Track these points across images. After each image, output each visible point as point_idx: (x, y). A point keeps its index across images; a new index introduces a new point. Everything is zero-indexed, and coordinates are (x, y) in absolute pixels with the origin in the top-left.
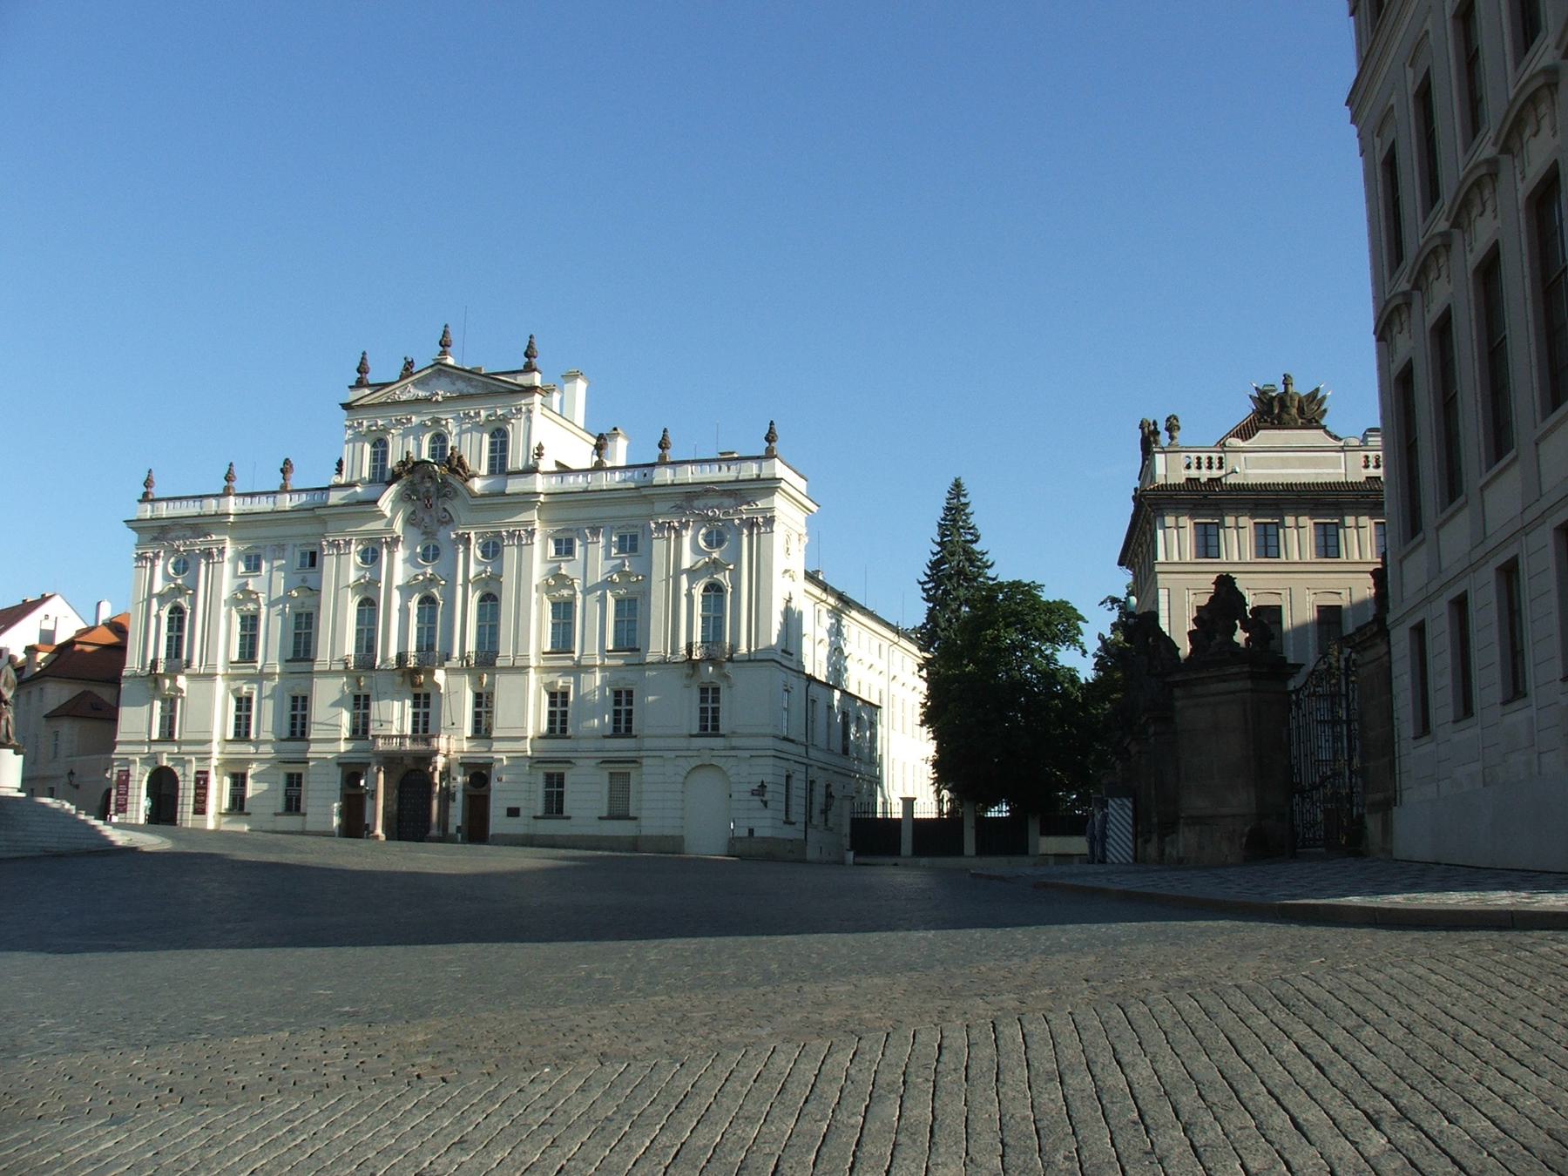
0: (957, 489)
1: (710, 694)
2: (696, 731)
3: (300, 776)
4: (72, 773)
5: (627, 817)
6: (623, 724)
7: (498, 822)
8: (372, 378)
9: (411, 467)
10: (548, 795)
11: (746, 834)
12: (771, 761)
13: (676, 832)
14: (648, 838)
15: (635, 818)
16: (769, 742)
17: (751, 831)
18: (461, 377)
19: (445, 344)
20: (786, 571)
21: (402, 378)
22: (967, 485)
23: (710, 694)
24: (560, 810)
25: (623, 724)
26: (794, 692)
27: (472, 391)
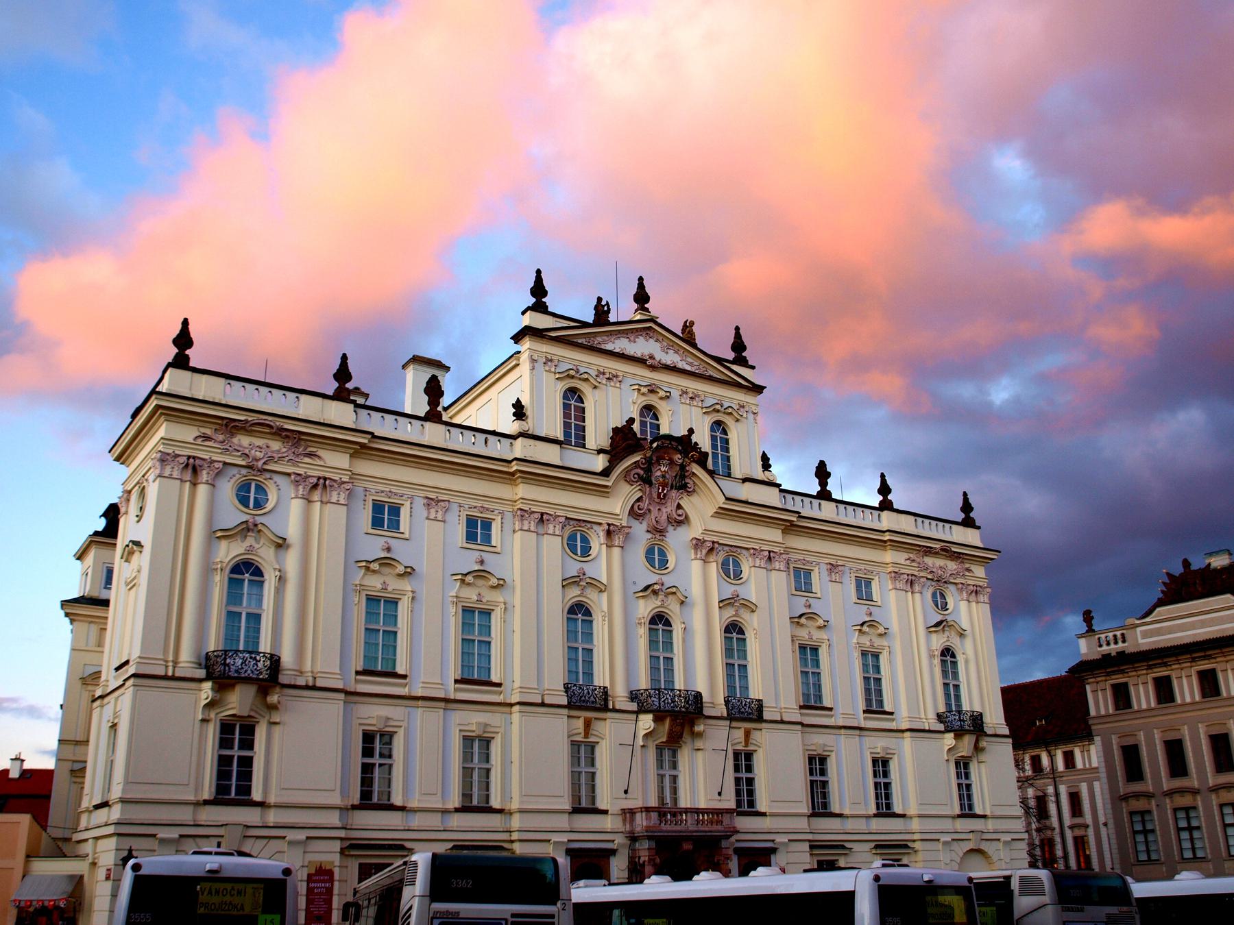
2: (957, 811)
19: (641, 298)
27: (688, 368)
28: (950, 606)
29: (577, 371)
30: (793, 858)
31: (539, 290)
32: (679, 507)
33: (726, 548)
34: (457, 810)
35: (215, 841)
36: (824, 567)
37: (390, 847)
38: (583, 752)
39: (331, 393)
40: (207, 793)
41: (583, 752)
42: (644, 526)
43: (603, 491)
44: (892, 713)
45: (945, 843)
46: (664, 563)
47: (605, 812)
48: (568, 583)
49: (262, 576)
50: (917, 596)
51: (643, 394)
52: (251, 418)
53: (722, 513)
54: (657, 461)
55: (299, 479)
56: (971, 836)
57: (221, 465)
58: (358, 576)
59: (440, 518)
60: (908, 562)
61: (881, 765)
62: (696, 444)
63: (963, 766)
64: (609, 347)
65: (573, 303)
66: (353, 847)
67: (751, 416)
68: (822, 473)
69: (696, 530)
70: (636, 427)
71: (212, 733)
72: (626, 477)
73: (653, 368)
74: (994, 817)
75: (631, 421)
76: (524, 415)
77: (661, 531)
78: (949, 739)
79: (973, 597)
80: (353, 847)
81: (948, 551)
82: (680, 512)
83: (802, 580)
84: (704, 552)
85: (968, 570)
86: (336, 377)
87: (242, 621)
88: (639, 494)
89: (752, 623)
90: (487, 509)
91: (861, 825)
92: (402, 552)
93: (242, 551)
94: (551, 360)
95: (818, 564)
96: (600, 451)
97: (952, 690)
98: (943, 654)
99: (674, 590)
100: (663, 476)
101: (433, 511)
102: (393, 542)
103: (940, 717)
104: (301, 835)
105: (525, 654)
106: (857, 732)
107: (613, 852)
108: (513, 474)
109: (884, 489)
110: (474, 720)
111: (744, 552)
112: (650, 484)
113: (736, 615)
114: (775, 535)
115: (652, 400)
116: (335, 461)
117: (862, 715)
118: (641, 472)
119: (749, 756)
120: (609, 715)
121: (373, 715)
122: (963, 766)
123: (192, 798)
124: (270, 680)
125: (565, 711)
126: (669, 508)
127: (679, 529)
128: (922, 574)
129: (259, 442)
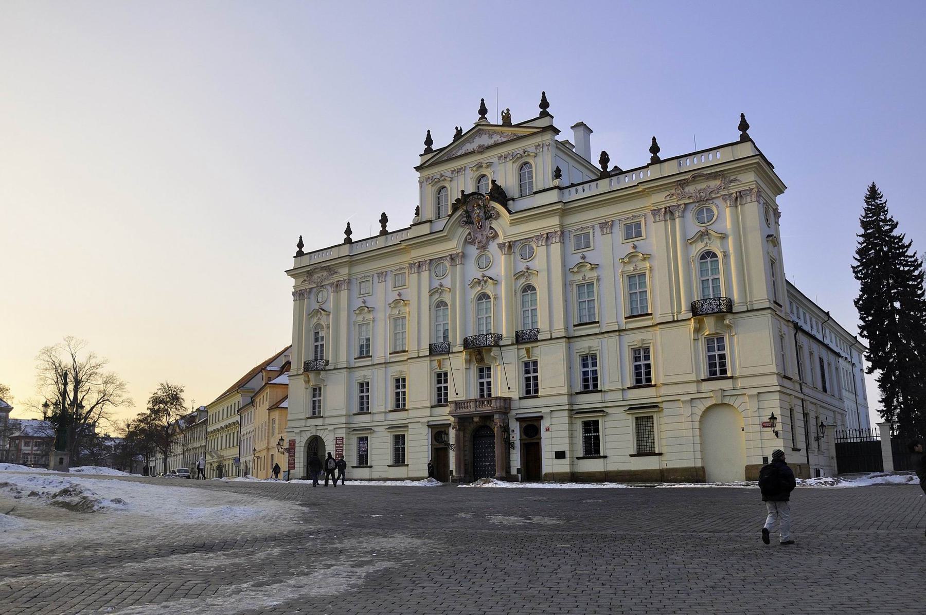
0: (873, 193)
1: (715, 343)
3: (403, 436)
5: (654, 454)
6: (643, 377)
7: (549, 464)
8: (434, 147)
9: (465, 199)
10: (587, 440)
12: (777, 396)
13: (699, 464)
15: (660, 454)
16: (774, 380)
18: (495, 132)
19: (483, 111)
20: (769, 236)
21: (454, 141)
22: (880, 188)
23: (715, 343)
24: (598, 451)
25: (643, 378)
26: (786, 338)
27: (505, 140)
29: (442, 176)
30: (554, 421)
31: (429, 141)
32: (491, 228)
34: (390, 411)
38: (441, 377)
40: (309, 414)
41: (441, 377)
45: (683, 402)
48: (432, 292)
52: (312, 267)
55: (331, 284)
56: (711, 394)
58: (354, 317)
60: (668, 198)
69: (501, 240)
71: (310, 392)
73: (481, 152)
74: (741, 377)
75: (463, 192)
85: (732, 181)
86: (346, 233)
87: (319, 350)
89: (539, 283)
95: (594, 226)
98: (703, 257)
106: (617, 334)
107: (450, 424)
110: (394, 371)
112: (472, 223)
114: (553, 222)
115: (484, 171)
119: (535, 363)
121: (360, 375)
123: (304, 417)
128: (679, 203)
129: (320, 275)
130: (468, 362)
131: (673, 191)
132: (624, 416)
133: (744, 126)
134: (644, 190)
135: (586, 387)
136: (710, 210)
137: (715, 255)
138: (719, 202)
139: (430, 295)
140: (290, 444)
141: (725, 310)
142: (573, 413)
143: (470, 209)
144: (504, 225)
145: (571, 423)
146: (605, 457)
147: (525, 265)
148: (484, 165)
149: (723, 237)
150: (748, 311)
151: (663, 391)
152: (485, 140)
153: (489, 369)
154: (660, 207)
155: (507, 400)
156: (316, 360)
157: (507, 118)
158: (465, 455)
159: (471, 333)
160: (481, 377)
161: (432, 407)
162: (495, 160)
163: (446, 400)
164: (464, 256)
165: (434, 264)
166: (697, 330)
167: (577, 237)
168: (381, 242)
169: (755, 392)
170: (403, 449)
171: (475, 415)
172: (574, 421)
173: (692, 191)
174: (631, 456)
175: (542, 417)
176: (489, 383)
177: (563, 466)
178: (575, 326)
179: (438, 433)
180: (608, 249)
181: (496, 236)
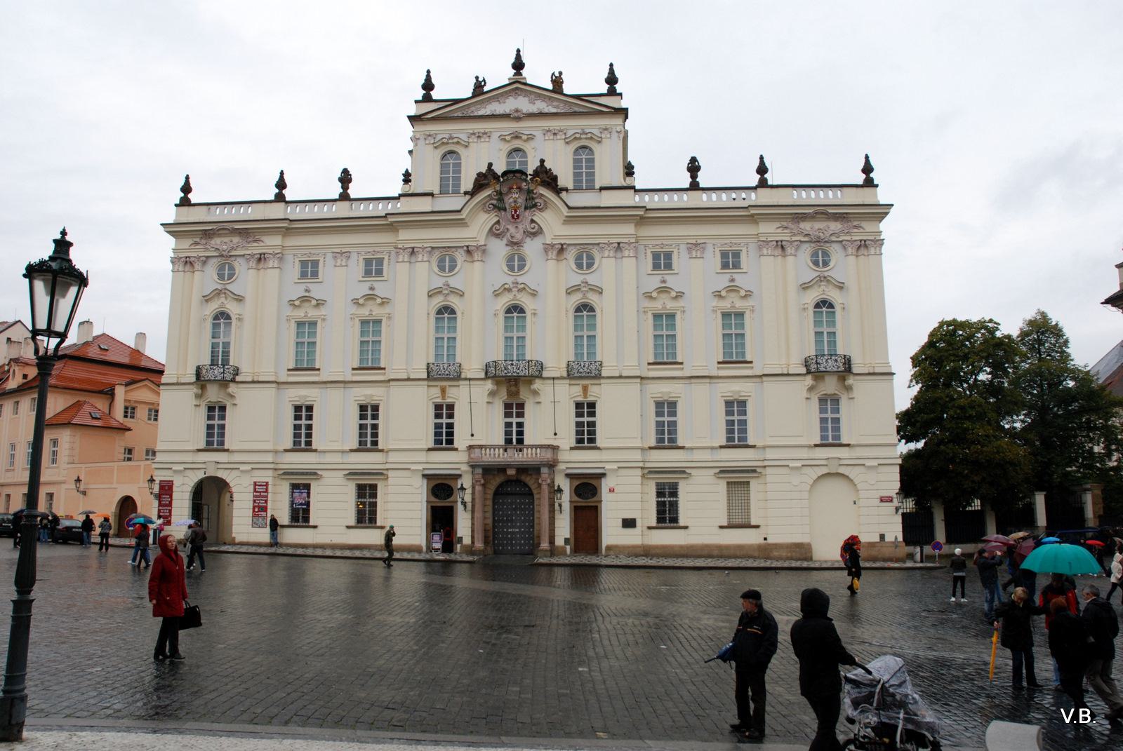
4: (78, 480)
5: (750, 526)
7: (612, 534)
10: (661, 505)
11: (877, 539)
12: (897, 469)
14: (777, 546)
15: (757, 527)
17: (882, 537)
18: (539, 96)
19: (518, 65)
21: (475, 95)
24: (674, 520)
27: (554, 110)
28: (832, 264)
29: (451, 138)
31: (428, 86)
32: (533, 221)
33: (578, 247)
35: (203, 471)
36: (683, 248)
37: (307, 474)
38: (444, 410)
39: (273, 198)
41: (444, 410)
42: (505, 241)
43: (462, 223)
44: (751, 362)
46: (521, 267)
47: (456, 449)
49: (230, 319)
50: (790, 259)
51: (508, 141)
53: (569, 221)
54: (515, 191)
57: (204, 259)
58: (289, 311)
59: (344, 264)
60: (779, 230)
61: (736, 407)
62: (550, 170)
63: (829, 403)
64: (481, 112)
65: (453, 87)
66: (284, 474)
67: (615, 135)
68: (694, 168)
70: (499, 168)
71: (203, 411)
72: (484, 207)
73: (518, 119)
75: (490, 165)
76: (410, 181)
77: (516, 244)
78: (809, 380)
79: (863, 251)
80: (284, 474)
81: (821, 212)
82: (533, 225)
83: (663, 261)
84: (555, 253)
85: (856, 227)
88: (496, 219)
90: (378, 252)
91: (706, 455)
92: (317, 292)
93: (217, 306)
94: (430, 135)
96: (466, 193)
97: (825, 337)
98: (817, 306)
99: (522, 286)
100: (515, 202)
101: (339, 261)
102: (311, 286)
103: (807, 364)
104: (248, 467)
105: (408, 346)
106: (708, 380)
107: (460, 476)
108: (391, 224)
109: (762, 170)
111: (596, 247)
112: (505, 210)
113: (584, 297)
114: (629, 229)
116: (272, 242)
117: (716, 365)
118: (494, 202)
119: (592, 405)
120: (461, 383)
122: (829, 403)
124: (230, 379)
125: (426, 383)
126: (525, 224)
127: (535, 238)
128: (794, 238)
129: (226, 239)
130: (492, 394)
131: (785, 224)
132: (712, 480)
133: (868, 169)
134: (752, 216)
135: (660, 440)
136: (826, 254)
137: (831, 306)
138: (836, 247)
139: (430, 296)
140: (161, 487)
141: (846, 369)
142: (648, 472)
143: (505, 190)
144: (552, 222)
145: (642, 484)
146: (686, 528)
147: (582, 278)
148: (525, 137)
149: (841, 287)
150: (870, 374)
151: (770, 454)
152: (523, 104)
153: (521, 406)
154: (770, 239)
155: (555, 448)
156: (214, 363)
157: (557, 82)
158: (485, 518)
159: (496, 353)
160: (508, 415)
161: (429, 450)
162: (538, 134)
163: (450, 442)
164: (484, 251)
165: (437, 254)
166: (811, 389)
167: (656, 256)
168: (341, 210)
169: (875, 463)
170: (374, 505)
171: (510, 466)
172: (645, 482)
173: (808, 228)
174: (721, 527)
175: (603, 475)
176: (520, 425)
177: (632, 538)
178: (649, 364)
179: (441, 488)
180: (697, 277)
181: (537, 233)
